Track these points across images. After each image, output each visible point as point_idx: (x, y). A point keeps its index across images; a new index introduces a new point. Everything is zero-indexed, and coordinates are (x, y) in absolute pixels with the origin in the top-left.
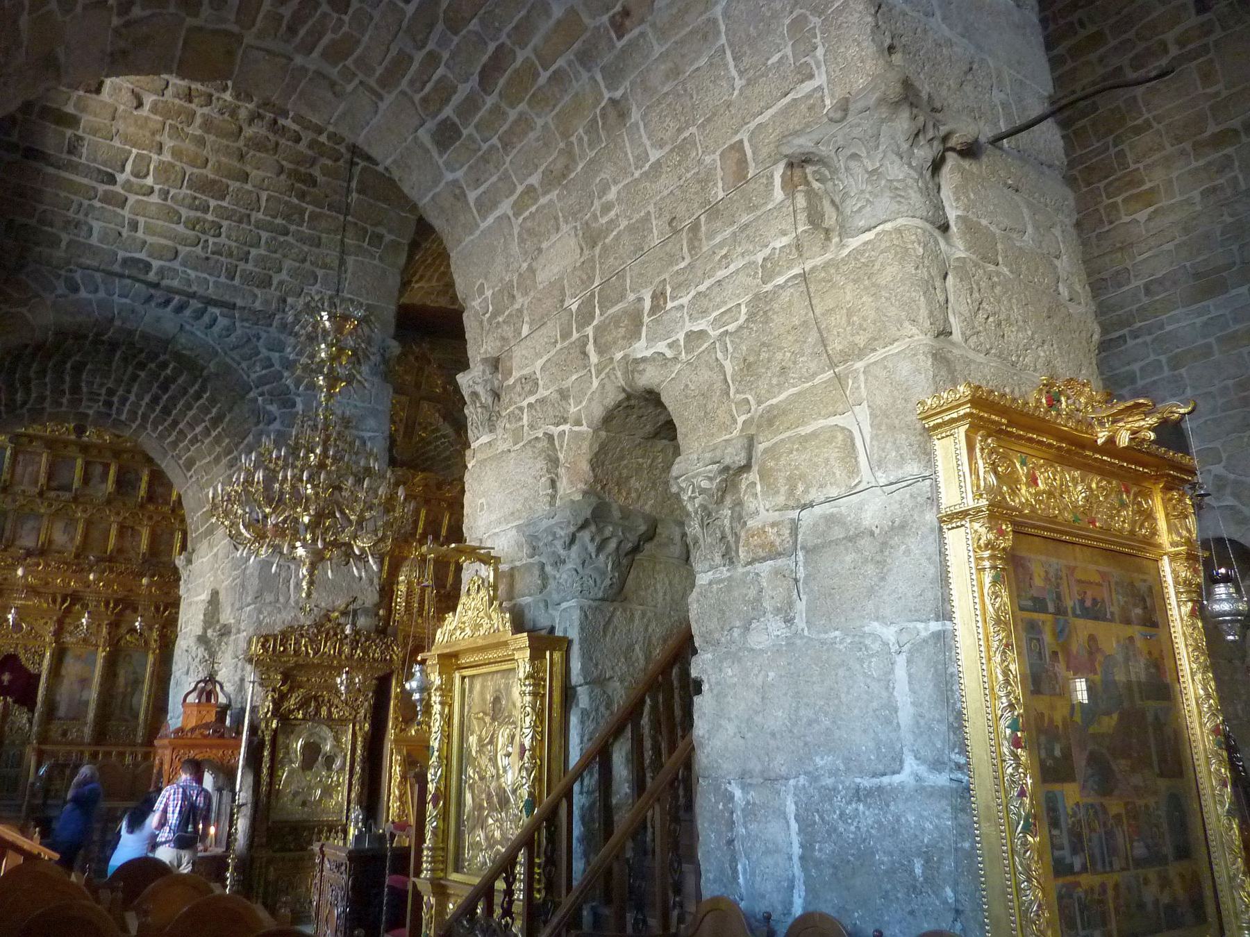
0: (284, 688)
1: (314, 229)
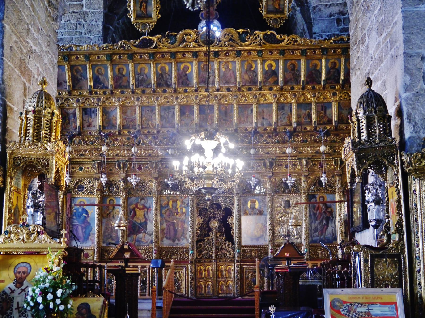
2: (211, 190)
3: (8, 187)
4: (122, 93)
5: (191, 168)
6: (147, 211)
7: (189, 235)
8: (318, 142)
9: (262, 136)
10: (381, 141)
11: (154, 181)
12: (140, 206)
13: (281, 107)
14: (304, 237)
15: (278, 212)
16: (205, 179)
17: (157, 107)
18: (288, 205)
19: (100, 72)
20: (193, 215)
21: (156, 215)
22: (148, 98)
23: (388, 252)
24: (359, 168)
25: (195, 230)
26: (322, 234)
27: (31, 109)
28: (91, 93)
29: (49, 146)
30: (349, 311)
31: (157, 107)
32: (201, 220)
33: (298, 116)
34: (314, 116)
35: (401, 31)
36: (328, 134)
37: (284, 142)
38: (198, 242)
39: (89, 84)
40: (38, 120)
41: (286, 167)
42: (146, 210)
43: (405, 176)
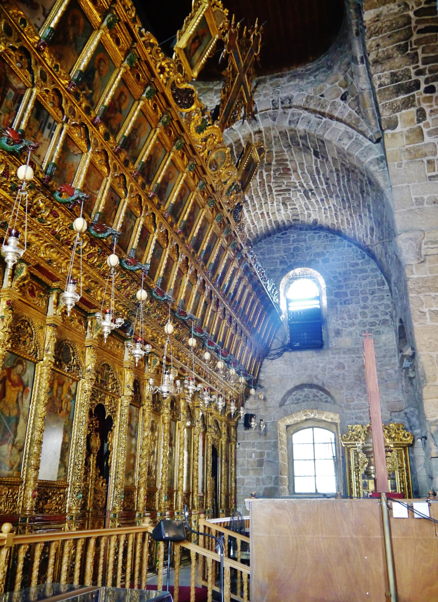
6: (23, 393)
19: (101, 68)
42: (21, 389)
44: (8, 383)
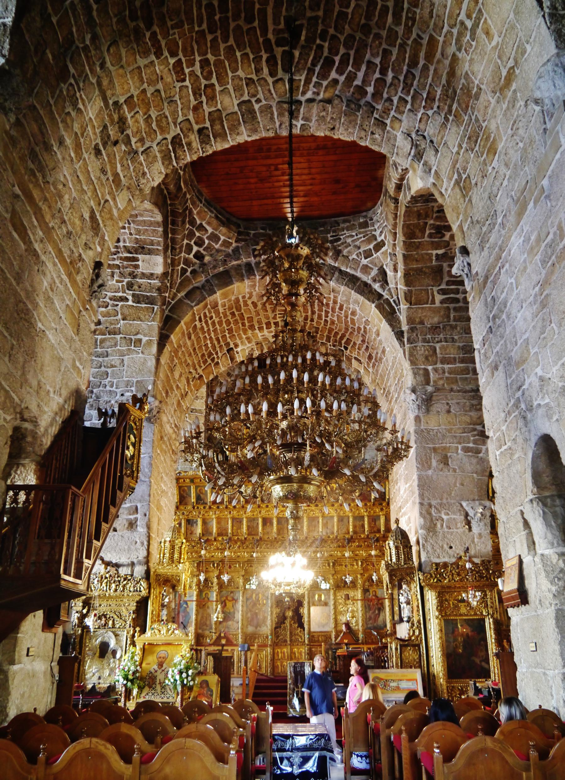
0: (85, 611)
1: (103, 348)
2: (289, 594)
3: (152, 595)
4: (218, 507)
5: (275, 579)
7: (269, 622)
8: (369, 547)
9: (326, 542)
10: (405, 564)
11: (241, 578)
12: (229, 598)
13: (341, 519)
14: (360, 624)
15: (340, 604)
16: (285, 585)
17: (245, 519)
18: (347, 597)
20: (272, 607)
21: (242, 606)
22: (238, 512)
23: (411, 643)
24: (391, 583)
25: (274, 619)
26: (375, 622)
27: (168, 539)
28: (194, 508)
29: (181, 566)
30: (385, 686)
31: (245, 519)
32: (278, 610)
33: (355, 527)
34: (366, 526)
35: (417, 488)
36: (377, 540)
37: (343, 547)
38: (276, 628)
39: (193, 501)
40: (173, 547)
41: (346, 566)
43: (422, 588)
44: (227, 601)
